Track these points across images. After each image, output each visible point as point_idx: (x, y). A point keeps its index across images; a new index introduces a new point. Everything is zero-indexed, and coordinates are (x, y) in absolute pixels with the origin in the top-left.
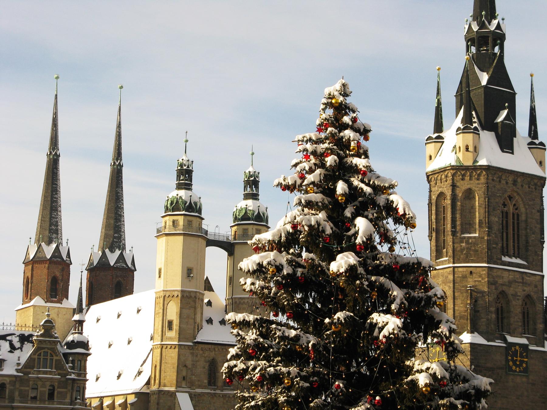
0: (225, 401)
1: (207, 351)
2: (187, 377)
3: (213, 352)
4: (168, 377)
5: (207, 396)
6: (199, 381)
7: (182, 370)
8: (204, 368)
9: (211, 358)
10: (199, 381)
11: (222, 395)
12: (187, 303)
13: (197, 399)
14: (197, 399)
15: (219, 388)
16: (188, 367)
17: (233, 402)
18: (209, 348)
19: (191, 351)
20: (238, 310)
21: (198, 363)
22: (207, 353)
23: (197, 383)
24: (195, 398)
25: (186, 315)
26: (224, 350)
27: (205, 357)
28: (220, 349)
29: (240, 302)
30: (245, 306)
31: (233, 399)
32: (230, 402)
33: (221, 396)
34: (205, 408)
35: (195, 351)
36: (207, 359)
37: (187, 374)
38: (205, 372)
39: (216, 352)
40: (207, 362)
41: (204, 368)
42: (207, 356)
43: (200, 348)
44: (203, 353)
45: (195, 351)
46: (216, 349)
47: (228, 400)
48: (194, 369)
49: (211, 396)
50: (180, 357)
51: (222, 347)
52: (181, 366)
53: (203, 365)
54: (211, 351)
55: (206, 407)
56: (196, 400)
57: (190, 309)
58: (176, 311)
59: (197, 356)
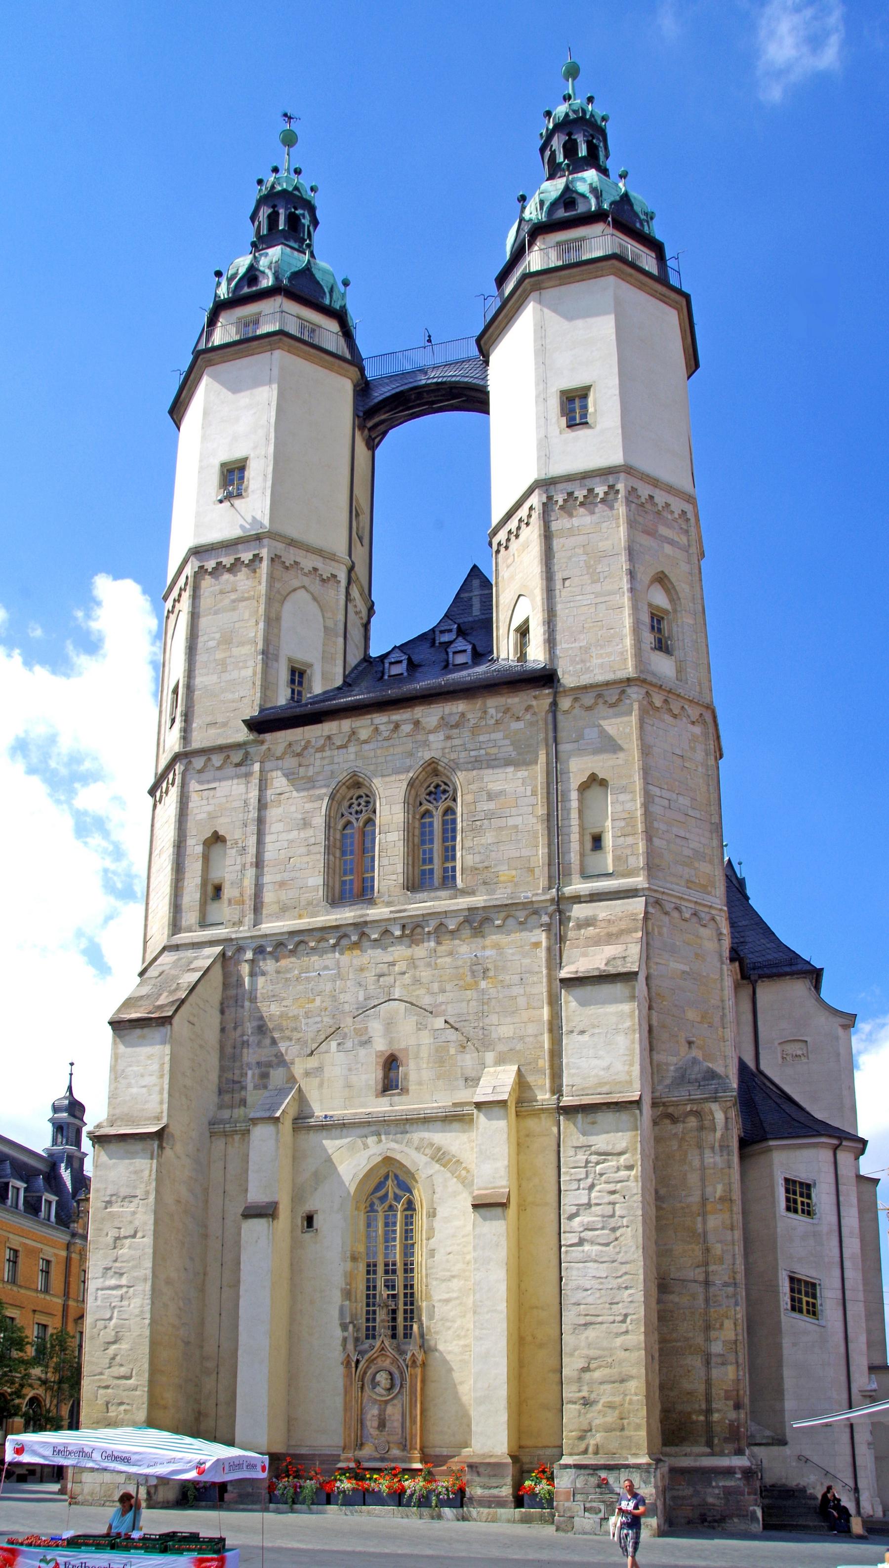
8: (306, 824)
10: (282, 884)
12: (222, 592)
22: (317, 763)
25: (218, 636)
32: (451, 954)
38: (312, 841)
39: (366, 747)
41: (306, 824)
42: (318, 773)
46: (364, 734)
51: (397, 716)
53: (300, 816)
54: (339, 748)
57: (234, 609)
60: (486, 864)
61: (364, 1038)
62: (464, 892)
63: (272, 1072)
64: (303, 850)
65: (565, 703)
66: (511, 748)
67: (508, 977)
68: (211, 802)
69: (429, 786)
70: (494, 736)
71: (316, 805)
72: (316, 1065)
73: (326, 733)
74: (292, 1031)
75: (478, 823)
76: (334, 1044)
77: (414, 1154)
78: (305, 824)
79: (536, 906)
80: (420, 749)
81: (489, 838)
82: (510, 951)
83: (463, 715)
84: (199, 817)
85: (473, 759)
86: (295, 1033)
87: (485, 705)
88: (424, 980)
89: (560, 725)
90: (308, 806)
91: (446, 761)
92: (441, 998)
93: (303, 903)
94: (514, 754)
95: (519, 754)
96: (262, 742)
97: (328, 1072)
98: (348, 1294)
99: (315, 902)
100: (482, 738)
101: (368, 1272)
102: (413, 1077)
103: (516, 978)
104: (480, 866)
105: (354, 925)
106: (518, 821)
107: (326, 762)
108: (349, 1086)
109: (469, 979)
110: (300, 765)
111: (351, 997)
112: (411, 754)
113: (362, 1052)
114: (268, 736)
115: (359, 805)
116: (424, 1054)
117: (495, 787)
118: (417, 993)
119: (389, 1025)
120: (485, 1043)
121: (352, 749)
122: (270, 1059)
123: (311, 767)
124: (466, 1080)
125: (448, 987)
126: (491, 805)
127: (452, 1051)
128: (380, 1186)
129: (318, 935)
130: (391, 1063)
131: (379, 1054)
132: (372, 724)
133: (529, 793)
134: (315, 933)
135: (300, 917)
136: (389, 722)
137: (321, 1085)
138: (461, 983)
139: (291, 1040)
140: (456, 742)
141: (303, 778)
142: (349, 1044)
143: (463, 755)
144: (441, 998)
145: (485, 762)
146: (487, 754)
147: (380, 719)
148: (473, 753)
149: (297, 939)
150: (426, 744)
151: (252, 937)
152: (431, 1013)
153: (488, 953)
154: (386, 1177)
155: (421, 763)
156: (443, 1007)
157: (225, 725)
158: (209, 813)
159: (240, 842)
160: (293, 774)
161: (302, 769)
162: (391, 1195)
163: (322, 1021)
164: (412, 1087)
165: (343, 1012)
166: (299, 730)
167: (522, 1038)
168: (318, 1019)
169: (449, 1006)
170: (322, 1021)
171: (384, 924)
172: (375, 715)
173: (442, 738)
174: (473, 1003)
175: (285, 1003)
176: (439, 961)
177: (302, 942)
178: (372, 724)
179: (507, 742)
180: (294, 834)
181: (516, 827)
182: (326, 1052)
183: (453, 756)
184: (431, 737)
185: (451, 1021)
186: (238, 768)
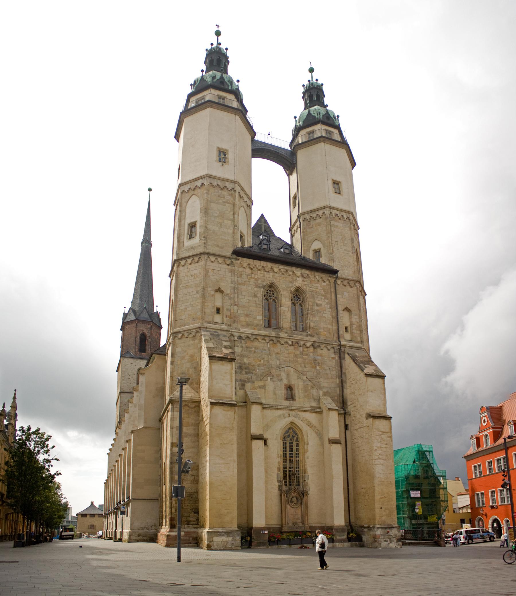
0: (298, 352)
1: (259, 270)
2: (223, 307)
3: (271, 274)
4: (189, 309)
5: (264, 342)
6: (247, 315)
7: (213, 296)
8: (255, 296)
9: (268, 282)
10: (247, 315)
11: (292, 342)
13: (244, 345)
14: (244, 345)
15: (285, 330)
16: (225, 291)
17: (311, 354)
18: (263, 267)
19: (229, 267)
20: (310, 228)
21: (244, 287)
22: (259, 274)
23: (242, 319)
24: (241, 342)
26: (291, 273)
27: (256, 279)
28: (282, 270)
29: (311, 217)
30: (319, 220)
31: (312, 349)
32: (307, 355)
33: (290, 343)
34: (260, 361)
35: (236, 268)
36: (259, 282)
37: (223, 302)
38: (258, 302)
40: (260, 287)
42: (259, 278)
43: (245, 265)
44: (252, 273)
45: (236, 268)
46: (276, 270)
47: (303, 351)
48: (236, 295)
49: (271, 342)
50: (209, 274)
51: (287, 268)
52: (210, 289)
54: (266, 272)
55: (263, 359)
56: (242, 347)
58: (200, 208)
59: (240, 276)
60: (317, 328)
61: (280, 378)
62: (310, 335)
63: (246, 384)
64: (254, 305)
65: (339, 282)
66: (322, 291)
67: (325, 367)
68: (217, 275)
69: (294, 295)
70: (317, 285)
71: (259, 289)
72: (263, 384)
73: (262, 265)
74: (253, 370)
75: (314, 313)
76: (269, 378)
77: (300, 421)
78: (255, 296)
79: (333, 346)
80: (294, 282)
81: (317, 318)
82: (325, 358)
83: (308, 275)
84: (213, 280)
85: (311, 291)
86: (254, 371)
87: (315, 274)
88: (299, 362)
89: (337, 288)
90: (256, 289)
91: (303, 288)
92: (305, 369)
93: (255, 325)
94: (324, 293)
95: (325, 294)
96: (238, 260)
97: (267, 388)
98: (279, 470)
99: (259, 325)
100: (314, 284)
101: (284, 462)
102: (297, 395)
103: (328, 368)
104: (315, 328)
105: (275, 337)
106: (325, 315)
107: (262, 275)
108: (275, 394)
109: (313, 364)
110: (252, 273)
111: (275, 362)
112: (291, 282)
113: (279, 383)
114: (240, 258)
115: (270, 294)
116: (300, 387)
117: (319, 302)
118: (297, 366)
119: (288, 375)
120: (320, 388)
121: (271, 274)
122: (246, 379)
123: (256, 275)
124: (314, 399)
125: (307, 366)
126: (317, 308)
127: (309, 388)
128: (287, 432)
129: (262, 337)
130: (290, 388)
131: (285, 385)
132: (278, 267)
133: (329, 308)
134: (261, 337)
135: (254, 329)
136: (284, 269)
137: (265, 392)
138: (311, 365)
139: (252, 373)
140: (306, 283)
141: (253, 278)
142: (275, 379)
143: (308, 288)
144: (305, 369)
145: (315, 293)
146: (315, 290)
147: (281, 267)
148: (311, 289)
149: (254, 337)
150: (296, 280)
151: (237, 332)
152: (302, 374)
153: (319, 358)
154: (289, 429)
155: (295, 286)
156: (306, 373)
157: (222, 248)
158: (217, 279)
159: (229, 295)
160: (250, 275)
161: (253, 275)
162: (291, 436)
163: (264, 369)
164: (297, 399)
165: (272, 367)
166: (252, 260)
167: (330, 388)
168: (263, 368)
169: (308, 372)
170: (264, 369)
171: (285, 339)
172: (279, 265)
173: (301, 280)
174: (315, 373)
175: (250, 359)
176: (304, 356)
177: (256, 338)
178: (278, 267)
179: (321, 288)
180: (251, 298)
181: (325, 317)
182: (266, 380)
183: (305, 288)
184: (298, 279)
185: (309, 378)
186: (228, 266)
